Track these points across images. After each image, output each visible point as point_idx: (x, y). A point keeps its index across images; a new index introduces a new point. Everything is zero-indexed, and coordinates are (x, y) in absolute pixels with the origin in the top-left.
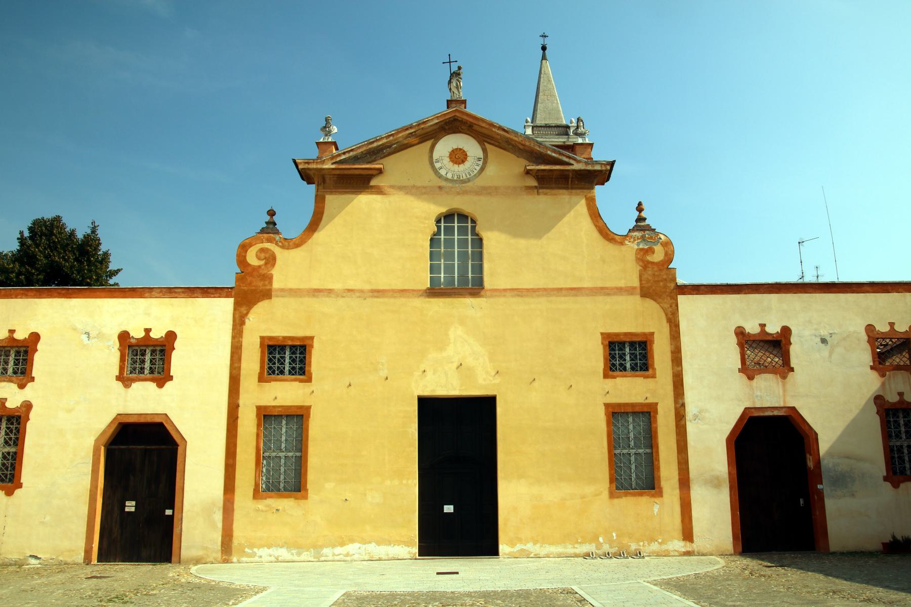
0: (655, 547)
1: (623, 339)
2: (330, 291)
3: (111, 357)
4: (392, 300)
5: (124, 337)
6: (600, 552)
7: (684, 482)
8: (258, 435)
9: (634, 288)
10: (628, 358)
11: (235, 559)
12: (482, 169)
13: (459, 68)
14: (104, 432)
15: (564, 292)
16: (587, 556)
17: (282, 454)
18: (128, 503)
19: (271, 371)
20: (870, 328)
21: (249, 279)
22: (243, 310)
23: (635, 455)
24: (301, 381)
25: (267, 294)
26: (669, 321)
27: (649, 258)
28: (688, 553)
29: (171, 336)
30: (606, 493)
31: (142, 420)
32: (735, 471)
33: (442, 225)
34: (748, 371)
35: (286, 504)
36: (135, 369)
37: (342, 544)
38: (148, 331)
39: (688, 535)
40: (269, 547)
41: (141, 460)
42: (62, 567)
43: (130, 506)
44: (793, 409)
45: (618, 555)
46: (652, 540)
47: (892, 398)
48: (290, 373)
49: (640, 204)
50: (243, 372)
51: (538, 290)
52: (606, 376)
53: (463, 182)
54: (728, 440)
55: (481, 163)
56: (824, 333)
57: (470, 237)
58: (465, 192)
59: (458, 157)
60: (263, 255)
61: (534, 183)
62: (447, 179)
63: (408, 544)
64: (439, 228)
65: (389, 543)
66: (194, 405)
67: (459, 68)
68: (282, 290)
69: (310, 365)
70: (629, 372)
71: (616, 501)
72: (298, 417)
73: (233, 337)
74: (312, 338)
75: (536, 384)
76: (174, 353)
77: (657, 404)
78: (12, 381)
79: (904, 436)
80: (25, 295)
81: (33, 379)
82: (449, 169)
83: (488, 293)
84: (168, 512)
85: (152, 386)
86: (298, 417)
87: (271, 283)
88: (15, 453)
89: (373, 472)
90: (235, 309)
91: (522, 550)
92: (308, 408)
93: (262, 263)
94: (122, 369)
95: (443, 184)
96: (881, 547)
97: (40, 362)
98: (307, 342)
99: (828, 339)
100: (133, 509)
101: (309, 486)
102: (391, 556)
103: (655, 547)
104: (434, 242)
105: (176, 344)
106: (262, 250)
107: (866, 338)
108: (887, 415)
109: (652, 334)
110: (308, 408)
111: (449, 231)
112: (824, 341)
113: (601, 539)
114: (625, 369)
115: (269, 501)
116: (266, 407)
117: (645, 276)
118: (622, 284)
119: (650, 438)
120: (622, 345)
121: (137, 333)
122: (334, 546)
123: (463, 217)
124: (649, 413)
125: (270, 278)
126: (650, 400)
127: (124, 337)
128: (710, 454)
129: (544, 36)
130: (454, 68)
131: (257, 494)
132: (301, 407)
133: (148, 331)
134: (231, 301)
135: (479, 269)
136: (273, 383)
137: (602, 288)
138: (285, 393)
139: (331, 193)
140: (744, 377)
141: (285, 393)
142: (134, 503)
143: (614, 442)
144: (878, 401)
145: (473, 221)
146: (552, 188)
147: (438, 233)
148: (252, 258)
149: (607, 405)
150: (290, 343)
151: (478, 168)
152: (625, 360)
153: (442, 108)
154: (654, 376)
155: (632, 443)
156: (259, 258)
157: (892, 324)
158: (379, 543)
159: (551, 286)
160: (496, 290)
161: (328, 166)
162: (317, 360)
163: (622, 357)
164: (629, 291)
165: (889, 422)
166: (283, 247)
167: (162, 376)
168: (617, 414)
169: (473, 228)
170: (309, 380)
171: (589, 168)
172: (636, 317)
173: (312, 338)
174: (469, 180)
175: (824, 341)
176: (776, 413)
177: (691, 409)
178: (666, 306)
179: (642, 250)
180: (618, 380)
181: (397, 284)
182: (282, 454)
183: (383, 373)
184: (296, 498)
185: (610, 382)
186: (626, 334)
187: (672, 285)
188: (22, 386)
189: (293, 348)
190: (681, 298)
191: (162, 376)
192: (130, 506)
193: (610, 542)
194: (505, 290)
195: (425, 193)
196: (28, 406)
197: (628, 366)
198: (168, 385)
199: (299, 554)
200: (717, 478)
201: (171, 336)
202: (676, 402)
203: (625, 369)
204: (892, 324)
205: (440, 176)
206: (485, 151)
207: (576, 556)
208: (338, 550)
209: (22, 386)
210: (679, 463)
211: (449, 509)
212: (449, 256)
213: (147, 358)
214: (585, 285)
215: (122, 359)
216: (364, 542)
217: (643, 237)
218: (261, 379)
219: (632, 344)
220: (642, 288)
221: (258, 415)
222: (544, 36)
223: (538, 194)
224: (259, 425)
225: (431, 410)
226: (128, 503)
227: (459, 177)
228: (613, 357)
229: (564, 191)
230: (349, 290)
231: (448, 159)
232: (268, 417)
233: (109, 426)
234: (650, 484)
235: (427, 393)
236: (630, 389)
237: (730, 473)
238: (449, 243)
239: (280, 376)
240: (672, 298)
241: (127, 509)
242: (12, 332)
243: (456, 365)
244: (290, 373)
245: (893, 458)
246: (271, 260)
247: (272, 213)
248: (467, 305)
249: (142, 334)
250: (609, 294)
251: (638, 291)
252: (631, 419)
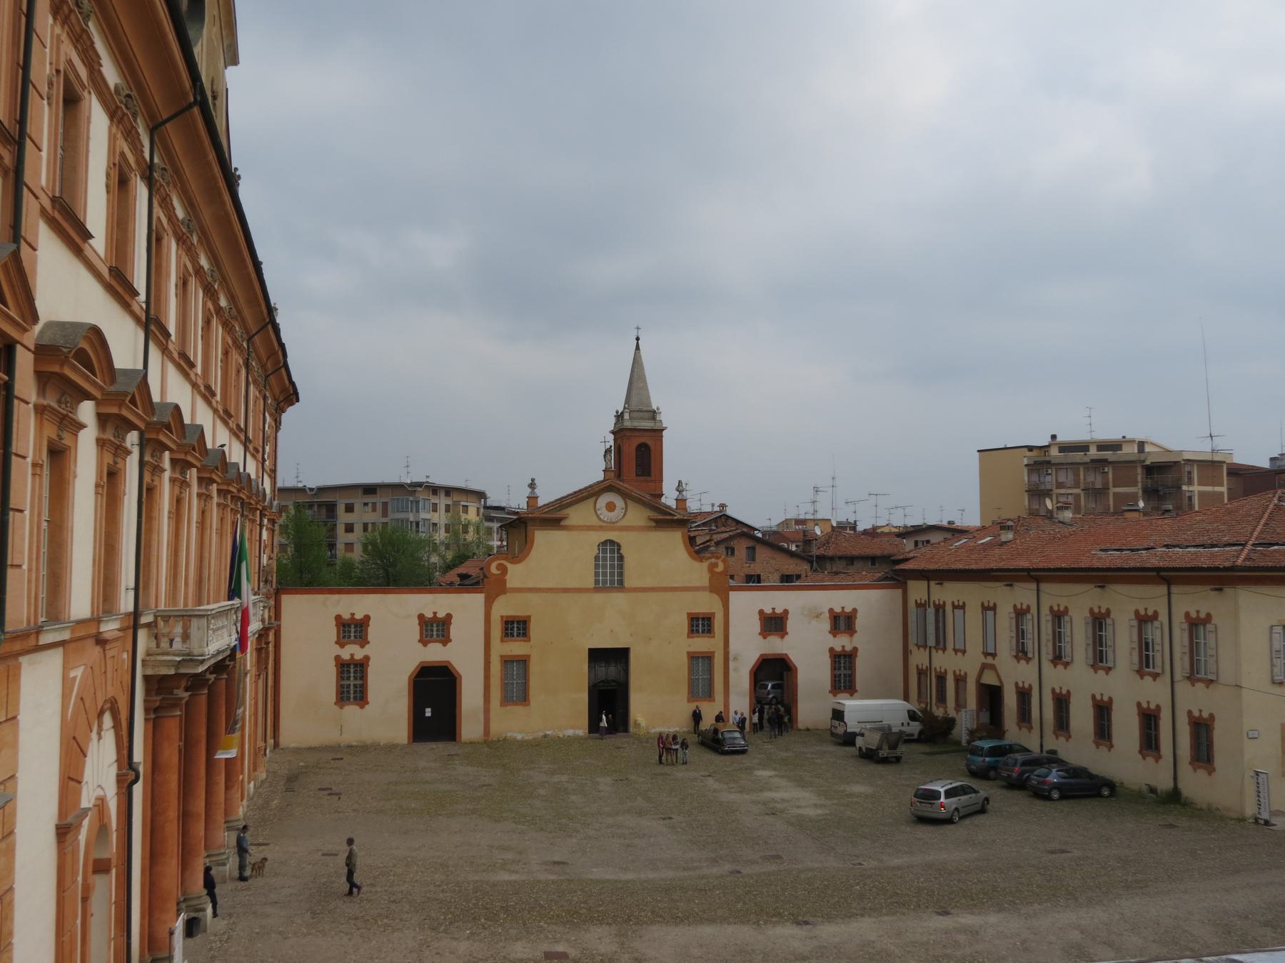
5: (421, 617)
35: (519, 710)
42: (391, 748)
43: (428, 712)
59: (611, 507)
66: (465, 653)
72: (523, 662)
82: (606, 515)
85: (440, 645)
86: (523, 662)
97: (372, 631)
104: (597, 558)
111: (604, 551)
118: (698, 584)
119: (710, 670)
120: (697, 619)
123: (612, 542)
125: (505, 581)
127: (421, 617)
133: (435, 613)
135: (621, 574)
138: (516, 648)
143: (691, 670)
148: (494, 569)
149: (688, 653)
162: (534, 629)
167: (445, 640)
168: (693, 657)
172: (706, 603)
185: (691, 640)
188: (362, 646)
190: (732, 594)
191: (445, 640)
192: (428, 712)
196: (367, 658)
209: (362, 646)
212: (605, 567)
213: (435, 629)
218: (502, 641)
225: (597, 656)
232: (507, 661)
236: (701, 644)
238: (605, 559)
242: (353, 614)
246: (504, 570)
248: (618, 599)
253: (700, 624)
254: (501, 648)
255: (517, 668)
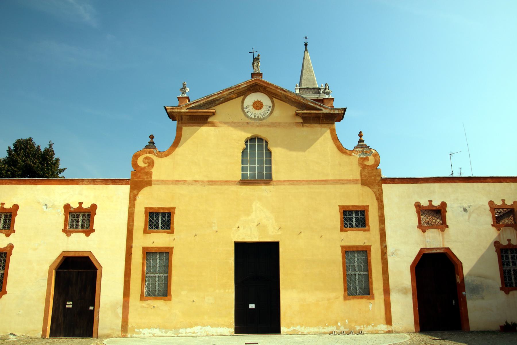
0: (370, 328)
1: (351, 209)
2: (185, 181)
3: (60, 219)
4: (220, 187)
5: (67, 207)
6: (339, 331)
7: (387, 291)
8: (143, 264)
9: (357, 180)
10: (354, 220)
11: (129, 335)
12: (271, 113)
13: (259, 56)
14: (55, 261)
15: (318, 182)
16: (331, 333)
17: (157, 275)
18: (68, 303)
19: (151, 227)
20: (491, 203)
21: (139, 174)
22: (135, 192)
23: (358, 275)
24: (168, 233)
25: (149, 183)
26: (378, 199)
27: (366, 163)
28: (389, 332)
29: (94, 207)
30: (342, 297)
31: (77, 255)
32: (415, 285)
33: (249, 144)
34: (423, 227)
35: (159, 304)
36: (73, 226)
37: (191, 327)
38: (81, 204)
39: (389, 321)
40: (149, 328)
41: (76, 278)
43: (69, 305)
44: (448, 249)
45: (349, 333)
46: (368, 324)
47: (505, 243)
48: (162, 228)
49: (361, 132)
50: (135, 228)
51: (303, 181)
52: (342, 230)
53: (261, 120)
54: (412, 267)
55: (270, 109)
56: (465, 205)
57: (264, 151)
58: (262, 126)
59: (258, 105)
60: (147, 161)
61: (301, 121)
62: (251, 118)
63: (228, 326)
64: (247, 146)
65: (218, 326)
66: (106, 246)
67: (259, 56)
68: (158, 181)
69: (173, 224)
70: (355, 228)
71: (348, 302)
72: (166, 254)
73: (129, 208)
74: (174, 208)
75: (302, 235)
76: (96, 217)
77: (370, 246)
78: (2, 232)
79: (511, 264)
80: (12, 184)
81: (14, 231)
82: (253, 113)
83: (275, 183)
84: (91, 308)
85: (82, 235)
86: (166, 254)
87: (151, 177)
88: (3, 274)
89: (209, 286)
90: (130, 192)
91: (294, 330)
92: (172, 248)
93: (146, 165)
94: (65, 225)
95: (249, 121)
96: (499, 328)
97: (19, 221)
98: (171, 211)
99: (467, 209)
100: (71, 306)
101: (172, 293)
102: (219, 334)
103: (370, 328)
104: (244, 153)
105: (97, 212)
106: (146, 158)
107: (489, 208)
108: (502, 252)
109: (368, 206)
110: (172, 248)
111: (253, 147)
112: (465, 210)
113: (339, 324)
114: (352, 226)
115: (149, 302)
116: (148, 248)
117: (364, 173)
118: (351, 178)
119: (367, 265)
120: (351, 212)
121: (75, 205)
122: (186, 328)
123: (260, 140)
124: (366, 251)
125: (150, 174)
126: (367, 244)
127: (67, 207)
128: (401, 275)
129: (306, 38)
130: (256, 55)
131: (142, 298)
132: (168, 248)
133: (81, 204)
134: (129, 186)
135: (269, 169)
136: (152, 234)
137: (339, 180)
138: (159, 240)
139: (186, 126)
140: (420, 231)
141: (159, 240)
142: (71, 303)
143: (346, 268)
144: (496, 245)
145: (266, 142)
146: (311, 123)
147: (246, 148)
148: (141, 162)
149: (342, 247)
150: (162, 211)
151: (269, 112)
152: (352, 221)
153: (249, 78)
154: (369, 230)
155: (357, 269)
156: (144, 163)
157: (503, 201)
158: (212, 326)
159: (310, 179)
160: (279, 181)
161: (184, 110)
162: (177, 221)
163: (351, 219)
164: (355, 182)
165: (502, 256)
166: (158, 156)
167: (88, 228)
169: (266, 146)
170: (173, 232)
171: (332, 112)
172: (358, 196)
173: (174, 208)
174: (264, 119)
175: (465, 210)
176: (438, 251)
177: (390, 249)
178: (376, 190)
179: (362, 158)
180: (349, 232)
181: (223, 177)
182: (157, 275)
183: (215, 228)
184: (165, 300)
185: (344, 234)
186: (353, 206)
187: (379, 179)
188: (8, 235)
189: (164, 214)
190: (384, 186)
191: (88, 228)
192: (69, 305)
193: (345, 325)
194: (284, 181)
195: (239, 126)
197: (354, 224)
198: (92, 235)
199: (166, 332)
200: (405, 289)
201: (94, 207)
202: (381, 245)
203: (352, 226)
204: (503, 201)
205: (248, 117)
206: (273, 102)
207: (325, 333)
208: (189, 330)
209: (8, 235)
210: (384, 280)
211: (252, 306)
212: (253, 162)
213: (81, 219)
214: (330, 178)
215: (66, 220)
216: (204, 325)
217: (362, 151)
218: (145, 232)
219: (356, 212)
220: (362, 180)
221: (143, 252)
222: (306, 38)
223: (303, 126)
224: (143, 258)
225: (242, 249)
226: (68, 303)
227: (258, 117)
228: (346, 219)
229: (318, 125)
230: (196, 181)
231: (252, 107)
232: (149, 253)
233: (58, 258)
234: (367, 292)
235: (240, 239)
236: (356, 238)
237: (412, 286)
238: (253, 154)
239: (156, 230)
240: (379, 185)
241: (67, 306)
243: (256, 223)
244: (162, 228)
245: (505, 277)
246: (151, 164)
247: (152, 137)
249: (78, 206)
250: (343, 184)
251: (360, 182)
252: (356, 255)
253: (354, 218)
254: (144, 240)
255: (159, 260)
